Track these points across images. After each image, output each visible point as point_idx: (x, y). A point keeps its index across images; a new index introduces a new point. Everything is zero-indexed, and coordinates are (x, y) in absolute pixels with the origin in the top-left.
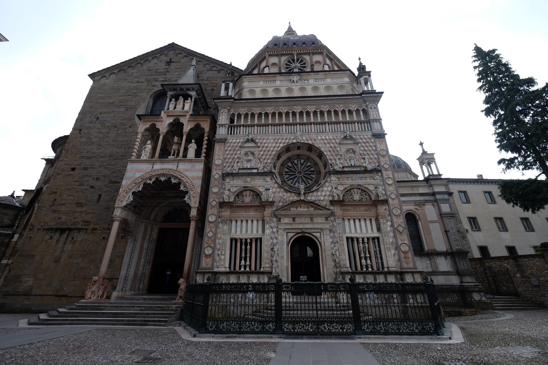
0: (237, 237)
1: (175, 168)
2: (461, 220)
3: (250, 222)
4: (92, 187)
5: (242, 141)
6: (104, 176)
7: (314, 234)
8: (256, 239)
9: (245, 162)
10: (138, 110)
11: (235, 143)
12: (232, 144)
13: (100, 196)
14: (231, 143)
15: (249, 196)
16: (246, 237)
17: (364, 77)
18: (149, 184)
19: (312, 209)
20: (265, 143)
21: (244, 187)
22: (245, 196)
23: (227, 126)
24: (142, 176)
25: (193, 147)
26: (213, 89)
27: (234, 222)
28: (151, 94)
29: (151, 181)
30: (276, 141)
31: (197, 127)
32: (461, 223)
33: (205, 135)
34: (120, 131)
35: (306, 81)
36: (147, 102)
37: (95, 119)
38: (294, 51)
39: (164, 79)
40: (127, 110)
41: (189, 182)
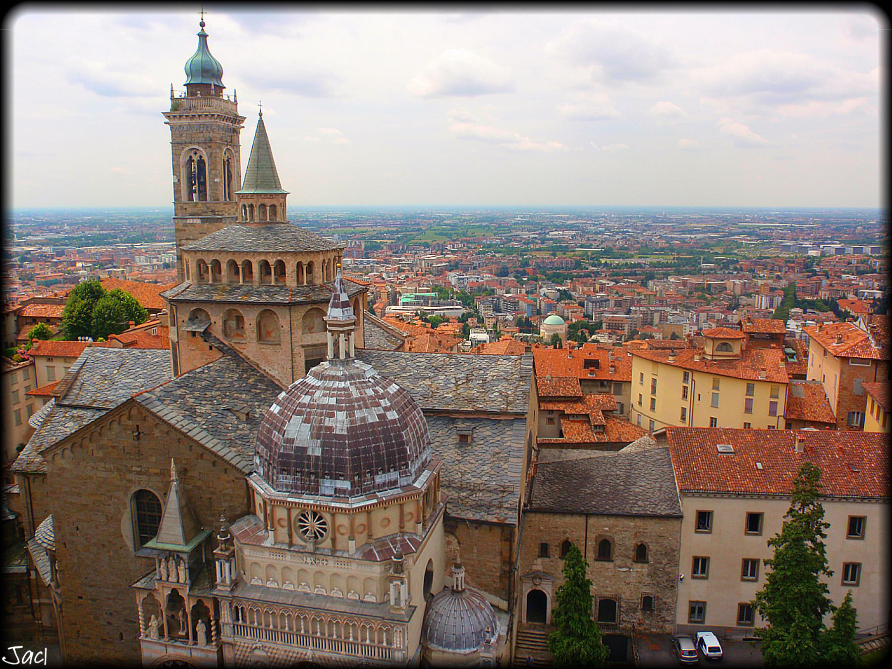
2: (679, 561)
4: (109, 623)
5: (250, 646)
6: (117, 612)
10: (122, 524)
11: (244, 647)
12: (241, 649)
13: (121, 634)
14: (240, 646)
17: (395, 583)
20: (275, 654)
23: (232, 626)
25: (201, 628)
26: (210, 498)
28: (129, 496)
30: (287, 653)
31: (200, 602)
32: (677, 565)
33: (211, 619)
34: (111, 553)
35: (325, 562)
36: (129, 509)
37: (75, 529)
38: (308, 506)
39: (139, 469)
40: (107, 519)
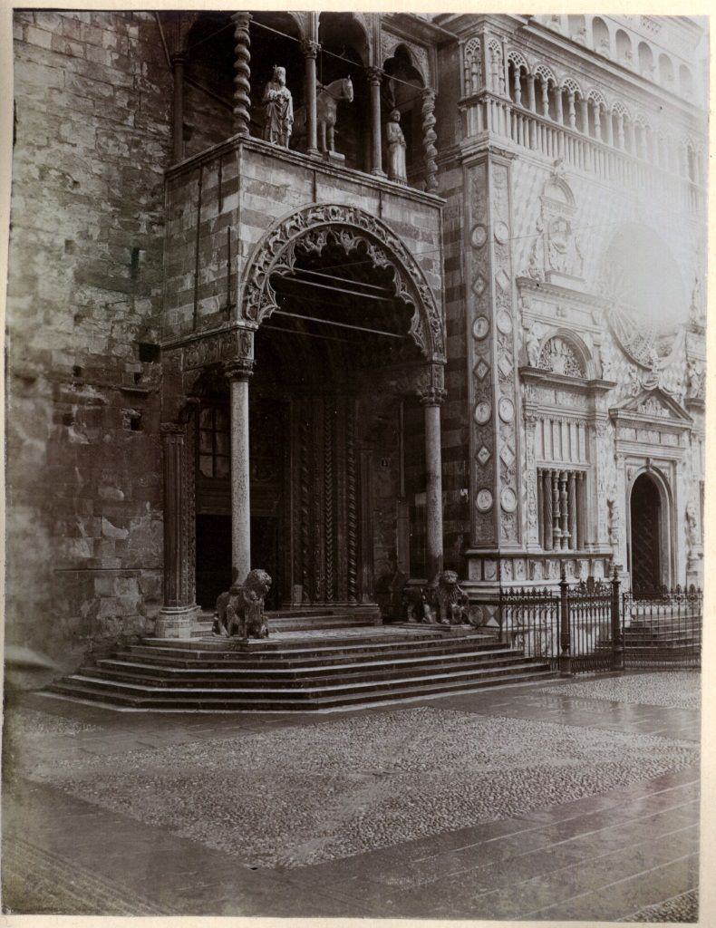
0: (548, 467)
1: (373, 212)
3: (565, 428)
7: (663, 471)
8: (578, 475)
9: (554, 252)
15: (562, 355)
16: (564, 468)
18: (314, 253)
19: (666, 413)
21: (561, 330)
22: (553, 355)
24: (292, 218)
27: (538, 425)
29: (315, 242)
41: (418, 273)
